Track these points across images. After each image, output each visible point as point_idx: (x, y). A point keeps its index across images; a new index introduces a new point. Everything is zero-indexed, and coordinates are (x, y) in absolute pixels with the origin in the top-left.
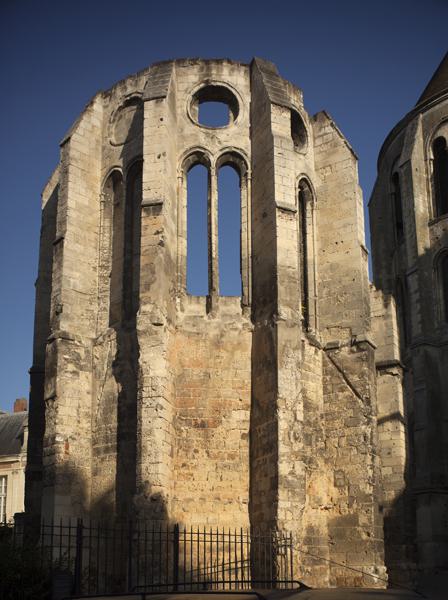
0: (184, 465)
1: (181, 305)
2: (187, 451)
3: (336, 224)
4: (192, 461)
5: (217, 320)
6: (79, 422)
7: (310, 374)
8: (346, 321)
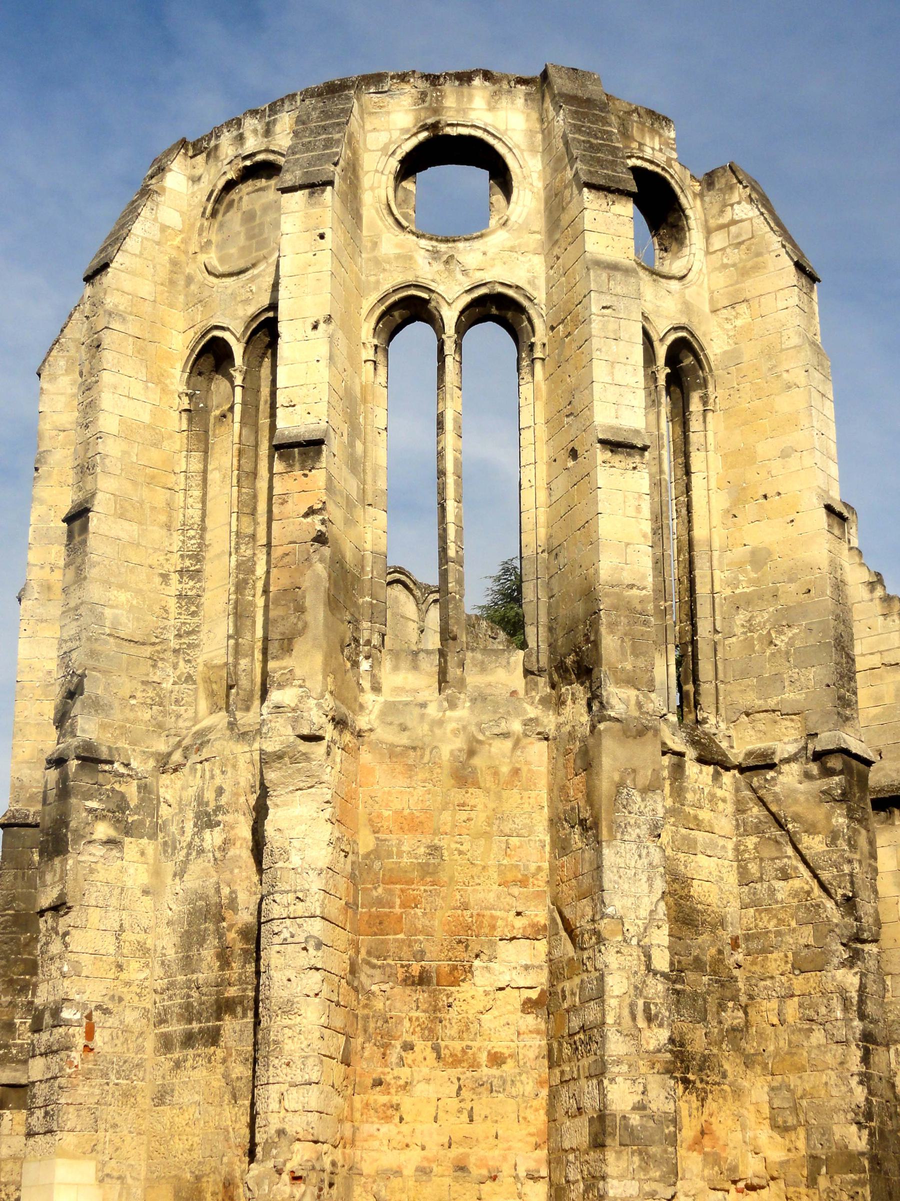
0: (378, 1083)
1: (373, 676)
2: (386, 1046)
3: (765, 448)
4: (397, 1071)
5: (463, 712)
6: (120, 967)
7: (700, 835)
8: (791, 696)
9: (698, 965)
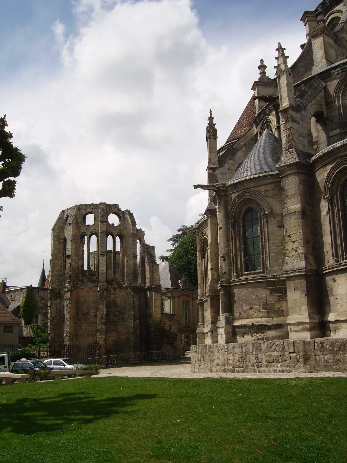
0: (79, 325)
6: (57, 312)
9: (117, 311)
